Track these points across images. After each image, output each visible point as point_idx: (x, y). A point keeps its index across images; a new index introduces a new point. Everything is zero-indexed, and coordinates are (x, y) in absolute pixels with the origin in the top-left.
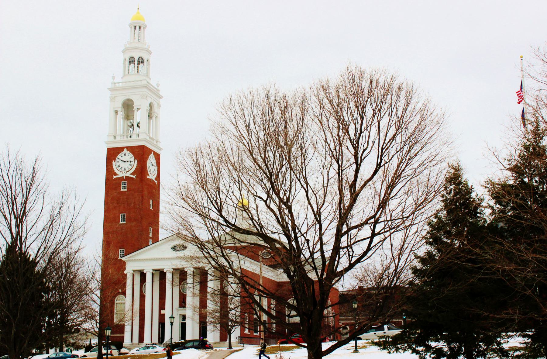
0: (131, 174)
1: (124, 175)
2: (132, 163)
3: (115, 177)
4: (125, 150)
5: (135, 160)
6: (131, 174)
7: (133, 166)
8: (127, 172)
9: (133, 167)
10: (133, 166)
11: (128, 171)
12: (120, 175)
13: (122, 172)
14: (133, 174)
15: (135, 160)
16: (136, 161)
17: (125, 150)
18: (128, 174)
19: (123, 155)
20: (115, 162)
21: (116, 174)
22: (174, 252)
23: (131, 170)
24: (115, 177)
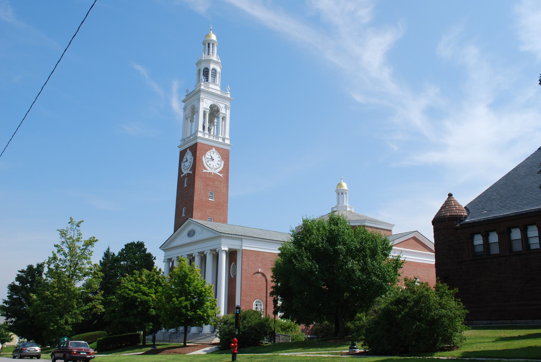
0: (219, 172)
2: (219, 163)
5: (222, 161)
8: (215, 169)
11: (217, 169)
12: (210, 170)
14: (219, 172)
18: (216, 172)
23: (218, 168)
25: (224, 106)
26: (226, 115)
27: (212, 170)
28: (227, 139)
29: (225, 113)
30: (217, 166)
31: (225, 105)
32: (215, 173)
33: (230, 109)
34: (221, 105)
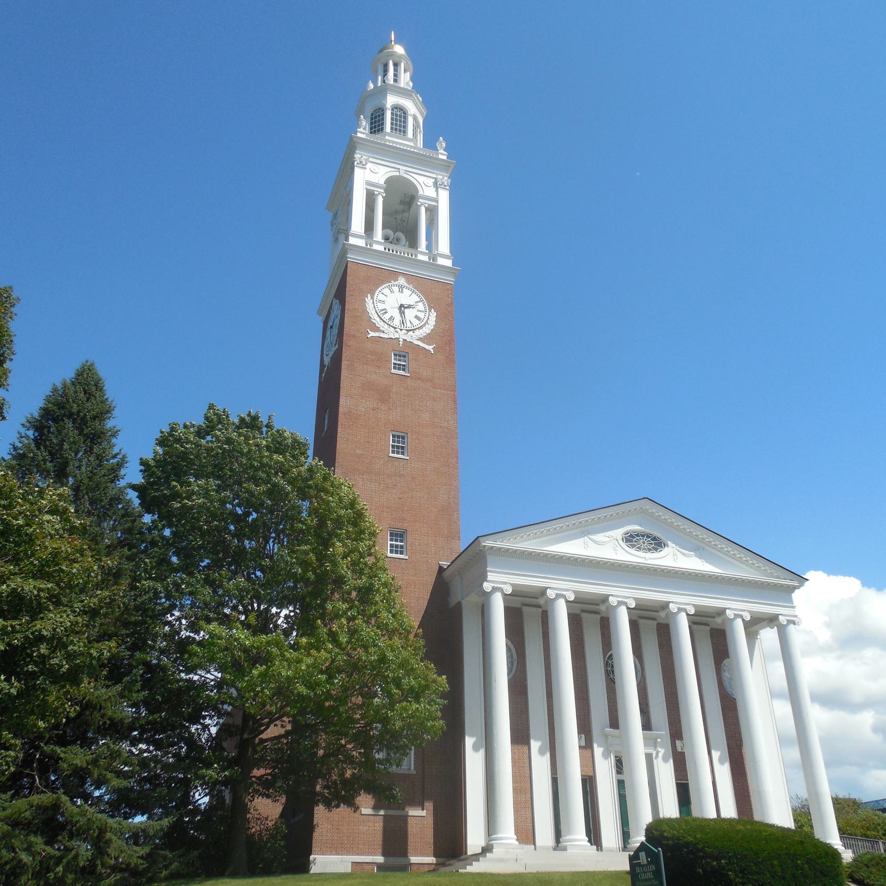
0: (420, 339)
1: (402, 335)
2: (421, 315)
3: (372, 334)
4: (402, 281)
5: (430, 311)
6: (420, 339)
7: (427, 322)
9: (424, 325)
10: (427, 322)
12: (390, 333)
13: (395, 328)
14: (426, 339)
15: (430, 311)
16: (433, 314)
17: (402, 281)
18: (413, 338)
19: (396, 289)
20: (372, 298)
21: (377, 329)
22: (632, 551)
24: (372, 334)
25: (431, 182)
26: (437, 202)
27: (397, 332)
28: (443, 256)
29: (436, 197)
30: (416, 322)
31: (434, 180)
32: (408, 340)
33: (448, 188)
34: (421, 179)
